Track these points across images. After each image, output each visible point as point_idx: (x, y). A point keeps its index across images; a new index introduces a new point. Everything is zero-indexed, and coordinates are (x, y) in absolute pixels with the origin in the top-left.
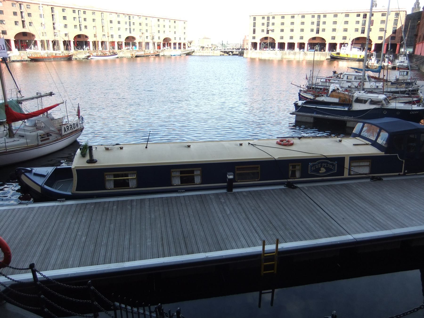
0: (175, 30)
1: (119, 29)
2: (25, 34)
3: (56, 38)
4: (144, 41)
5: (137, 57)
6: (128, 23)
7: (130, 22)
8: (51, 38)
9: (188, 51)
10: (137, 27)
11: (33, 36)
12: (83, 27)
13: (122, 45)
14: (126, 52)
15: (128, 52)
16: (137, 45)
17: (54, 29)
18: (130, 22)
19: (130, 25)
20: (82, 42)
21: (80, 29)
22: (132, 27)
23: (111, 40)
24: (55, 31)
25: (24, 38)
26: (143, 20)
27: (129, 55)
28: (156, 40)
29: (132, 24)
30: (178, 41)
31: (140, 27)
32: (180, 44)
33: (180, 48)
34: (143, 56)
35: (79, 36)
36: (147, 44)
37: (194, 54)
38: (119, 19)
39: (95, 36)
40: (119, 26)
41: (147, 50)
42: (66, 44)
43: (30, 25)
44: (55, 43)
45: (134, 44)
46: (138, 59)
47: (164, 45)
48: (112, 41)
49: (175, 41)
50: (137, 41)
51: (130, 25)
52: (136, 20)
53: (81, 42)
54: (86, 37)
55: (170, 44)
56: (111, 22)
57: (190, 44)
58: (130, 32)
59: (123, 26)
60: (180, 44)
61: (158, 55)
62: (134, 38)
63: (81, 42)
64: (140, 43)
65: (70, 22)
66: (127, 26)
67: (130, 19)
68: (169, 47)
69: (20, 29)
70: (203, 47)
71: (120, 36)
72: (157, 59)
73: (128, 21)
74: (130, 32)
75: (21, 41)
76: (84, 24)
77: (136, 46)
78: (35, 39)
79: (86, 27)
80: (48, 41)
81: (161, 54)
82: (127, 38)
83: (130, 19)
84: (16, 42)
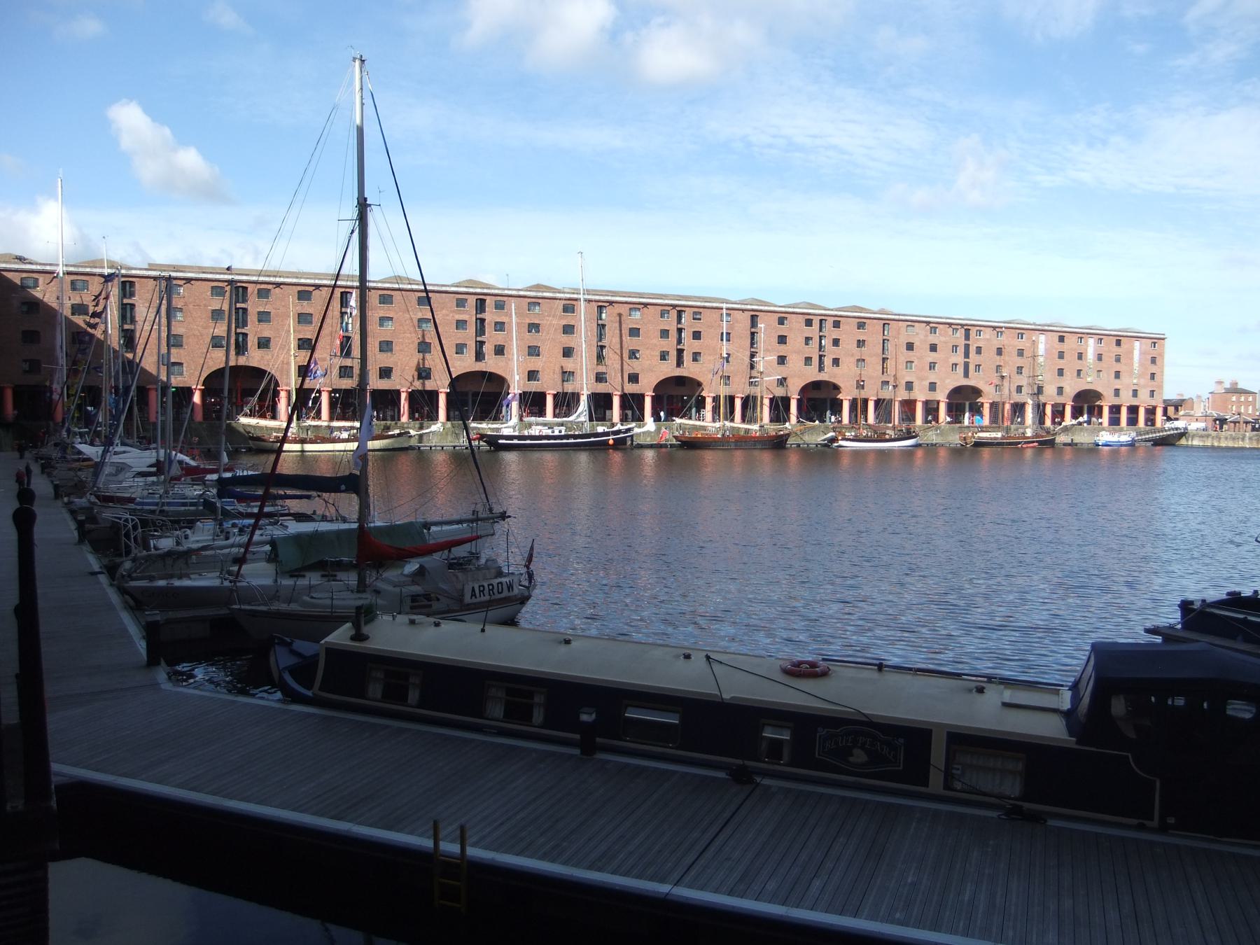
0: (1118, 367)
1: (932, 366)
2: (680, 381)
3: (756, 391)
4: (1008, 397)
5: (979, 444)
6: (961, 350)
7: (967, 347)
8: (740, 390)
9: (1163, 430)
10: (988, 359)
11: (699, 384)
12: (828, 361)
15: (953, 429)
16: (986, 410)
17: (752, 367)
18: (967, 347)
19: (967, 355)
20: (824, 401)
21: (821, 369)
23: (903, 395)
24: (754, 373)
26: (1004, 340)
27: (955, 439)
28: (1050, 396)
29: (972, 350)
30: (1126, 400)
31: (998, 360)
32: (1133, 410)
33: (1133, 421)
34: (999, 444)
35: (816, 385)
36: (1019, 408)
37: (1183, 442)
38: (933, 339)
39: (860, 386)
40: (932, 357)
42: (780, 408)
43: (695, 360)
45: (976, 410)
46: (986, 452)
47: (1077, 413)
49: (1116, 402)
50: (985, 401)
51: (967, 355)
52: (986, 339)
53: (819, 400)
54: (836, 388)
55: (1101, 408)
56: (910, 347)
57: (1177, 410)
58: (966, 375)
61: (1051, 443)
62: (977, 392)
63: (819, 400)
64: (994, 406)
66: (959, 358)
67: (967, 337)
69: (669, 369)
70: (1223, 421)
71: (933, 387)
72: (1048, 454)
73: (962, 342)
74: (966, 375)
75: (671, 397)
76: (831, 352)
78: (703, 394)
79: (836, 362)
80: (731, 399)
81: (1061, 439)
83: (967, 337)
84: (656, 401)
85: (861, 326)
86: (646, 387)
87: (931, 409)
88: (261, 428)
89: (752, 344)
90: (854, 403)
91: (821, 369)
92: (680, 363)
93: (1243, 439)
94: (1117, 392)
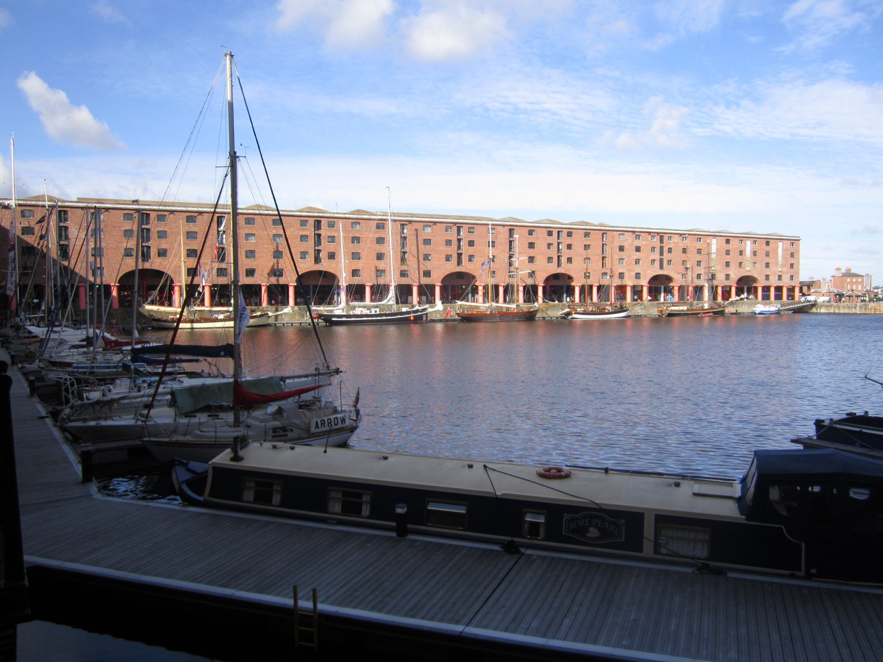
0: (767, 260)
1: (637, 261)
2: (460, 275)
3: (513, 281)
4: (691, 281)
5: (670, 315)
6: (657, 250)
7: (661, 248)
8: (502, 280)
9: (800, 302)
11: (474, 277)
12: (564, 260)
13: (641, 291)
14: (647, 308)
15: (653, 305)
16: (676, 292)
17: (510, 265)
18: (661, 248)
19: (661, 254)
20: (562, 287)
21: (559, 265)
22: (666, 256)
23: (617, 282)
24: (512, 269)
25: (457, 282)
26: (687, 243)
27: (654, 312)
28: (720, 280)
29: (665, 250)
30: (774, 282)
32: (779, 289)
33: (779, 297)
34: (685, 314)
35: (556, 276)
36: (698, 290)
37: (814, 310)
38: (638, 243)
39: (587, 276)
40: (637, 255)
41: (695, 302)
42: (530, 292)
43: (470, 260)
44: (508, 290)
45: (669, 291)
46: (676, 319)
47: (739, 292)
48: (619, 284)
49: (767, 283)
50: (675, 285)
51: (661, 254)
53: (558, 287)
54: (570, 278)
55: (756, 288)
56: (621, 249)
57: (809, 288)
58: (661, 267)
59: (646, 255)
60: (779, 289)
61: (721, 313)
62: (669, 279)
63: (558, 287)
65: (541, 251)
66: (656, 256)
67: (662, 241)
68: (751, 297)
69: (452, 267)
70: (841, 296)
71: (638, 276)
72: (720, 320)
73: (658, 245)
74: (661, 267)
75: (453, 287)
76: (566, 254)
77: (673, 295)
78: (477, 284)
79: (570, 260)
80: (496, 287)
81: (729, 310)
82: (655, 279)
83: (662, 241)
84: (443, 289)
85: (587, 235)
86: (436, 280)
87: (637, 292)
88: (161, 312)
89: (510, 249)
90: (582, 289)
91: (559, 265)
92: (459, 263)
93: (855, 308)
94: (767, 277)
